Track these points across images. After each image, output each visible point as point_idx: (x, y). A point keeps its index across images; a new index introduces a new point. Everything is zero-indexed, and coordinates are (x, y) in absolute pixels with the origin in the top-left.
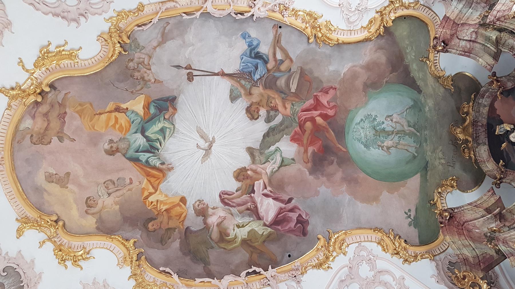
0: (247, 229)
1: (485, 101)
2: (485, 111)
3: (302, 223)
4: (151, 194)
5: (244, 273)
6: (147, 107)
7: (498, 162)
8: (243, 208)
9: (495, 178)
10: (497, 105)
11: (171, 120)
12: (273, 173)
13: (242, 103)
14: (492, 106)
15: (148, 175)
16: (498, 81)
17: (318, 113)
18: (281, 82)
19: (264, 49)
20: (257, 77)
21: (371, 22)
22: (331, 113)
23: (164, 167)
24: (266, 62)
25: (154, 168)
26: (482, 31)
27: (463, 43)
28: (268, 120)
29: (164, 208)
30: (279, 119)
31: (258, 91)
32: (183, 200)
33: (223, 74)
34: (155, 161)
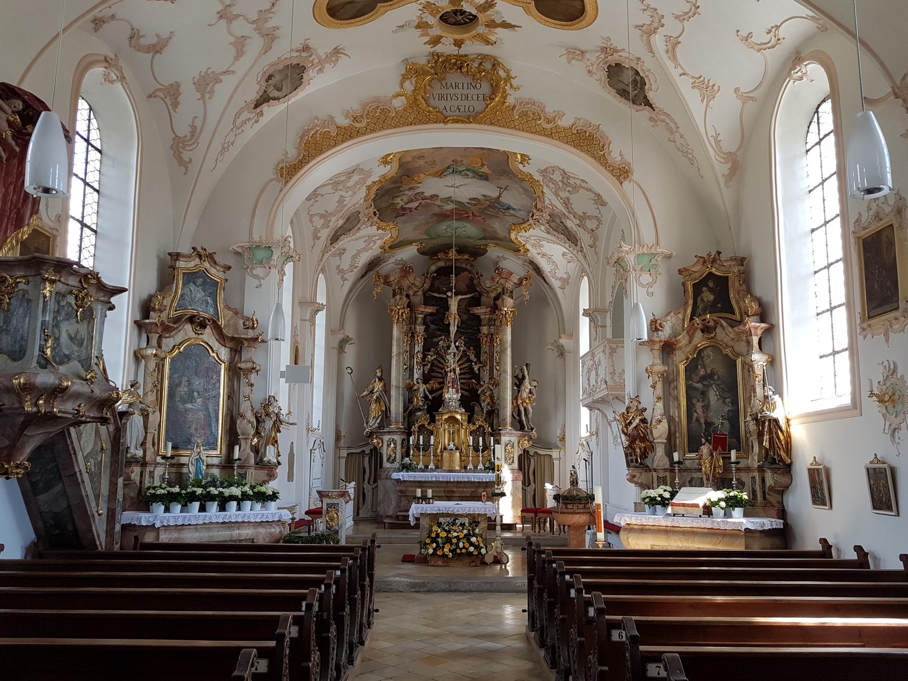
0: (400, 202)
1: (468, 267)
2: (464, 266)
3: (403, 215)
4: (425, 174)
5: (375, 210)
6: (483, 172)
7: (435, 273)
8: (413, 198)
9: (428, 274)
10: (466, 272)
11: (474, 177)
12: (435, 204)
13: (480, 197)
14: (466, 270)
15: (437, 172)
16: (478, 277)
17: (471, 215)
18: (491, 210)
19: (512, 211)
20: (496, 205)
21: (520, 241)
22: (470, 218)
23: (442, 175)
24: (504, 209)
25: (442, 173)
26: (502, 286)
27: (497, 280)
28: (467, 203)
29: (416, 179)
30: (470, 206)
31: (488, 203)
32: (420, 183)
33: (500, 196)
34: (446, 173)
